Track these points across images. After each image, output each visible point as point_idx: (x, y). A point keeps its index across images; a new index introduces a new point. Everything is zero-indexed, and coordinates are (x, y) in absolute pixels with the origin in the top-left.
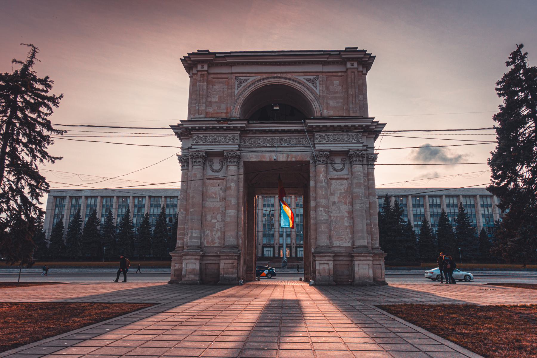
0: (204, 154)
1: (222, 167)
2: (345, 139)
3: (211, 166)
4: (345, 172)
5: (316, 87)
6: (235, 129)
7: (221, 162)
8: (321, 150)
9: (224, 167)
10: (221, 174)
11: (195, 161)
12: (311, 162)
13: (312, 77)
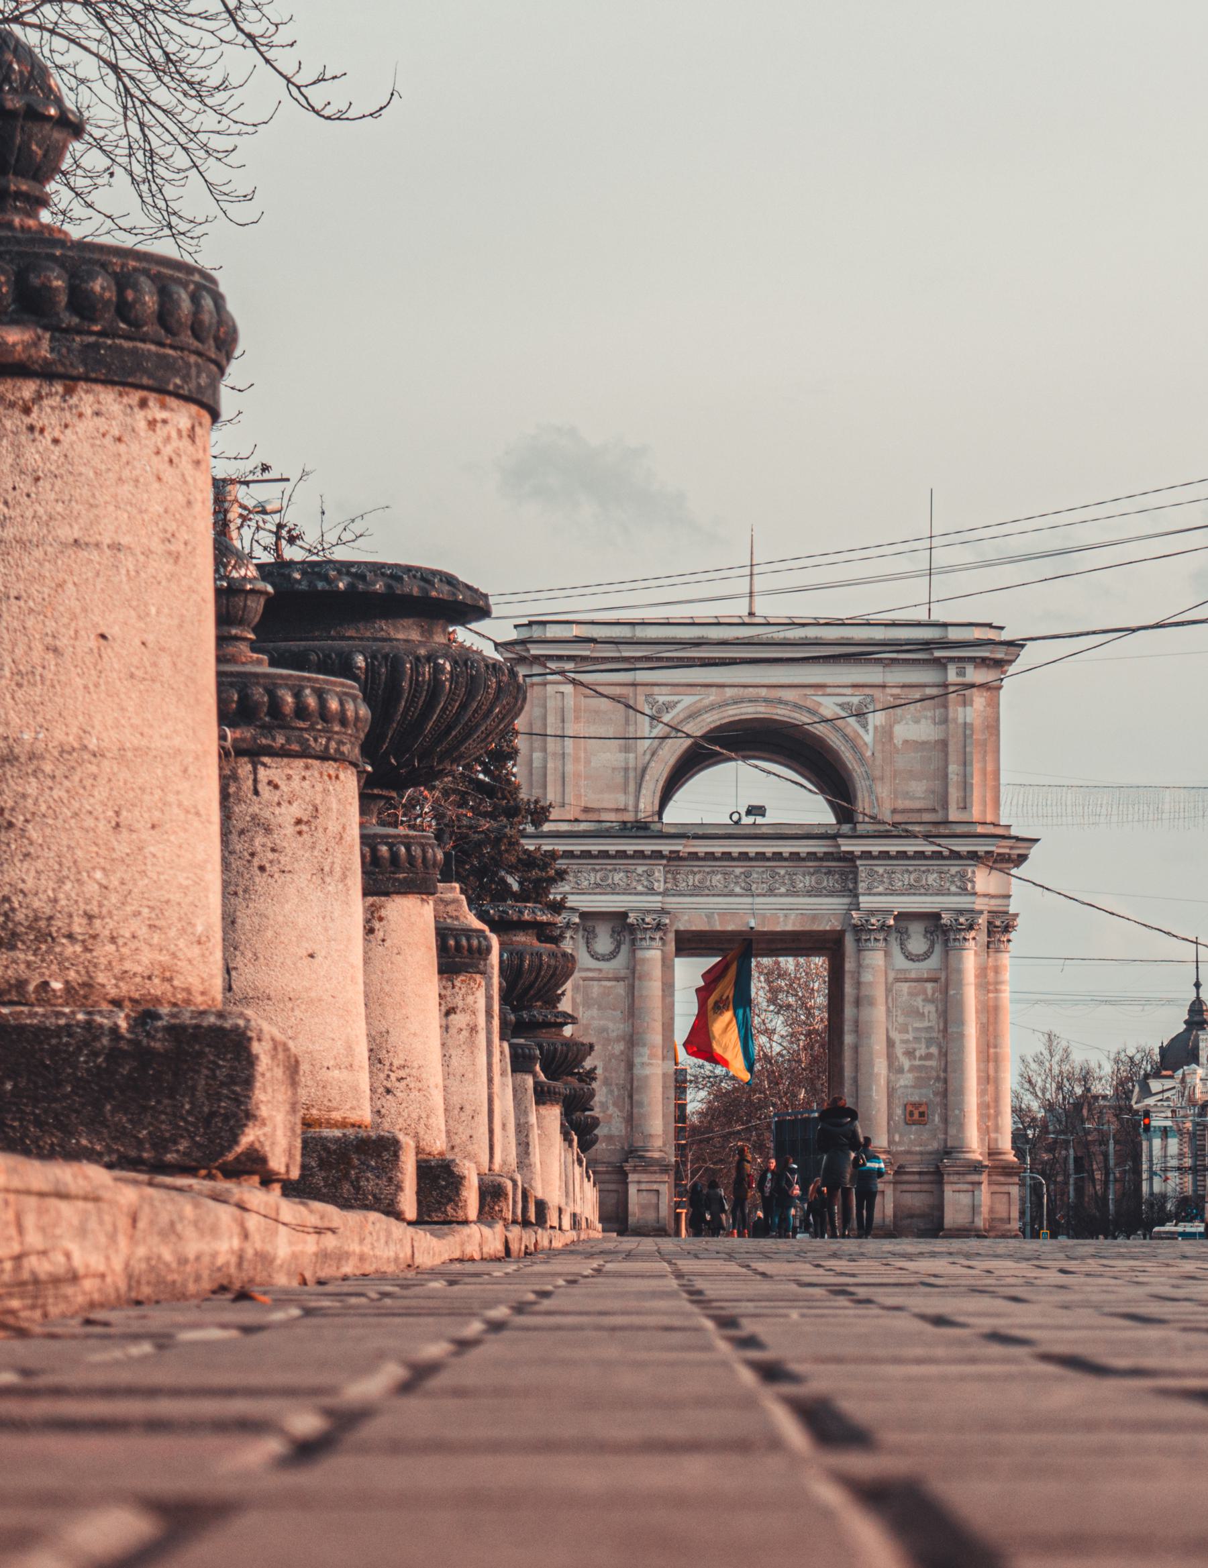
0: (577, 920)
1: (618, 947)
4: (934, 962)
5: (865, 726)
6: (657, 855)
8: (872, 912)
9: (624, 948)
12: (849, 940)
13: (855, 700)
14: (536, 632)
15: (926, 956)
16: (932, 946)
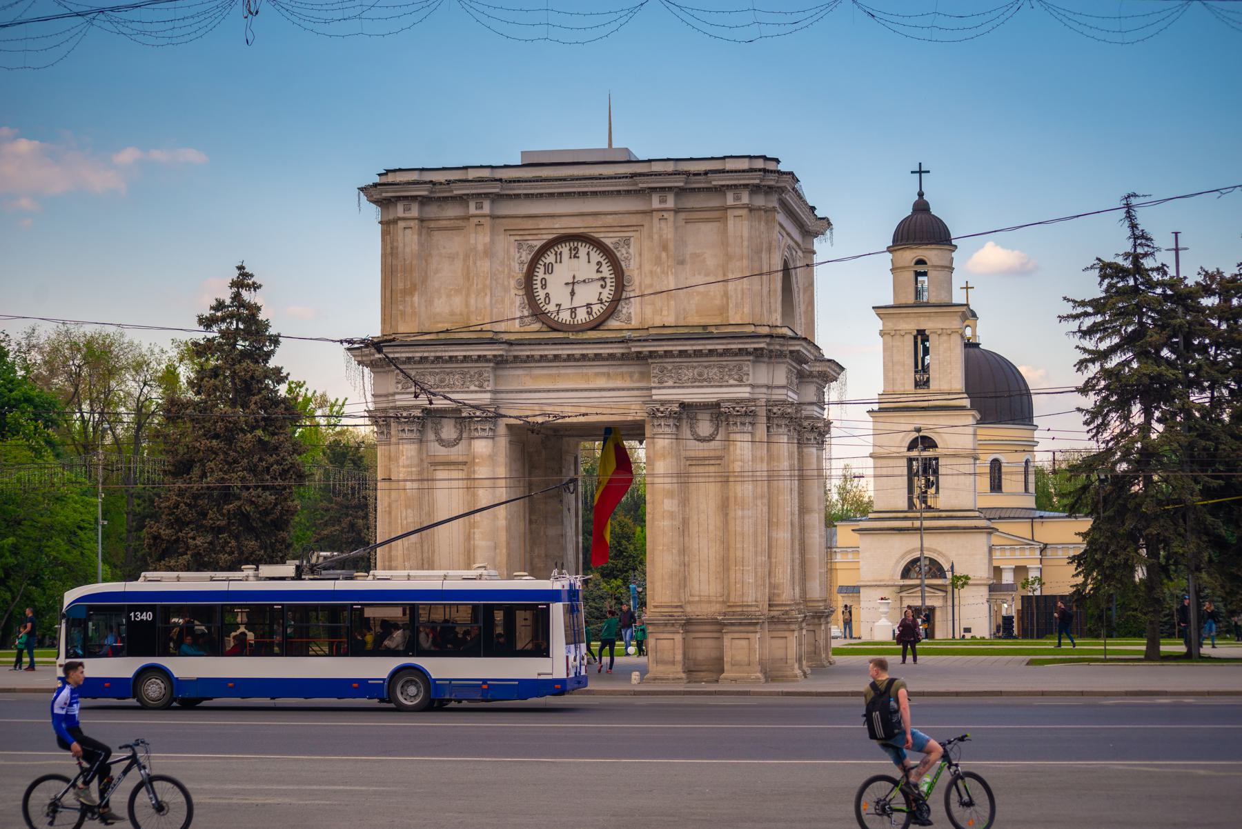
2: (714, 376)
3: (437, 433)
7: (458, 426)
8: (663, 403)
9: (465, 435)
10: (455, 453)
11: (403, 430)
14: (390, 178)
15: (711, 439)
16: (717, 429)
